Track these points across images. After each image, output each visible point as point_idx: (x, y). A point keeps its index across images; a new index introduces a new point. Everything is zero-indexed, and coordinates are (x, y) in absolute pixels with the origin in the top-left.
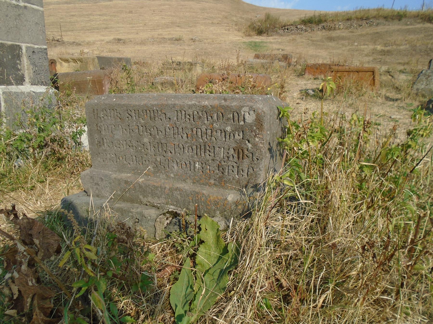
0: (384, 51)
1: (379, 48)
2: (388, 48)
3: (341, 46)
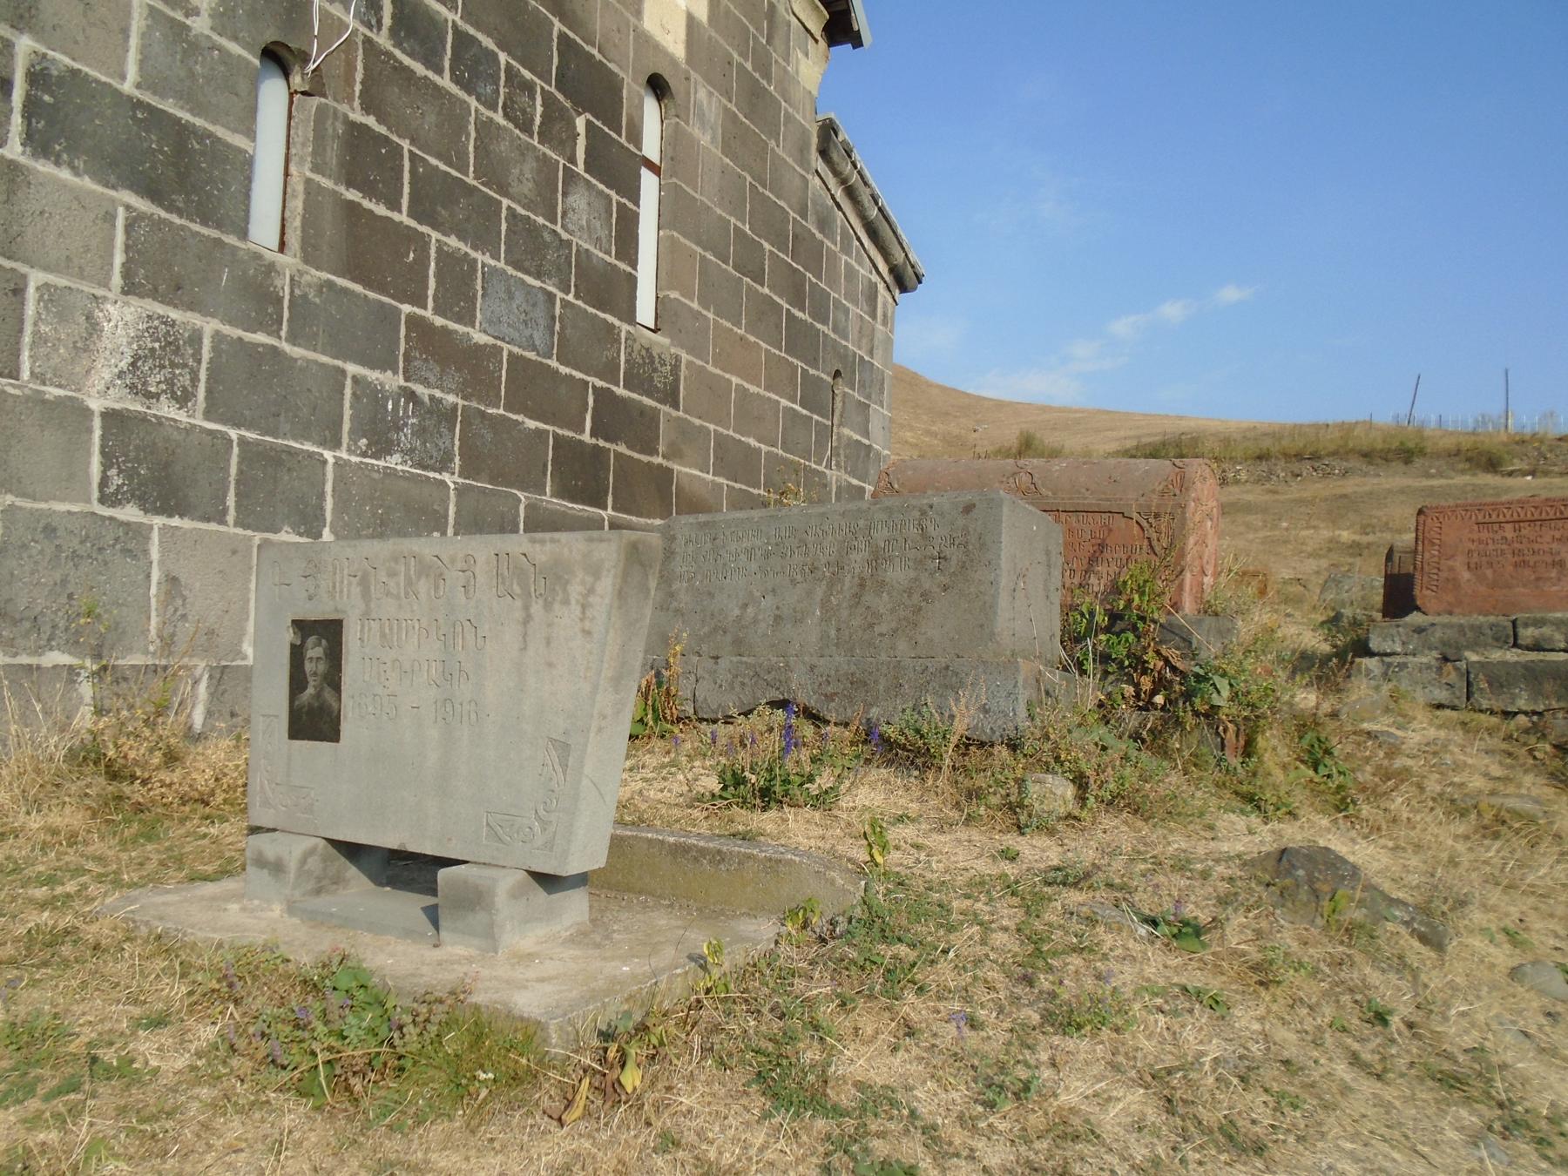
0: (1359, 544)
1: (1346, 536)
2: (1371, 538)
3: (1242, 529)
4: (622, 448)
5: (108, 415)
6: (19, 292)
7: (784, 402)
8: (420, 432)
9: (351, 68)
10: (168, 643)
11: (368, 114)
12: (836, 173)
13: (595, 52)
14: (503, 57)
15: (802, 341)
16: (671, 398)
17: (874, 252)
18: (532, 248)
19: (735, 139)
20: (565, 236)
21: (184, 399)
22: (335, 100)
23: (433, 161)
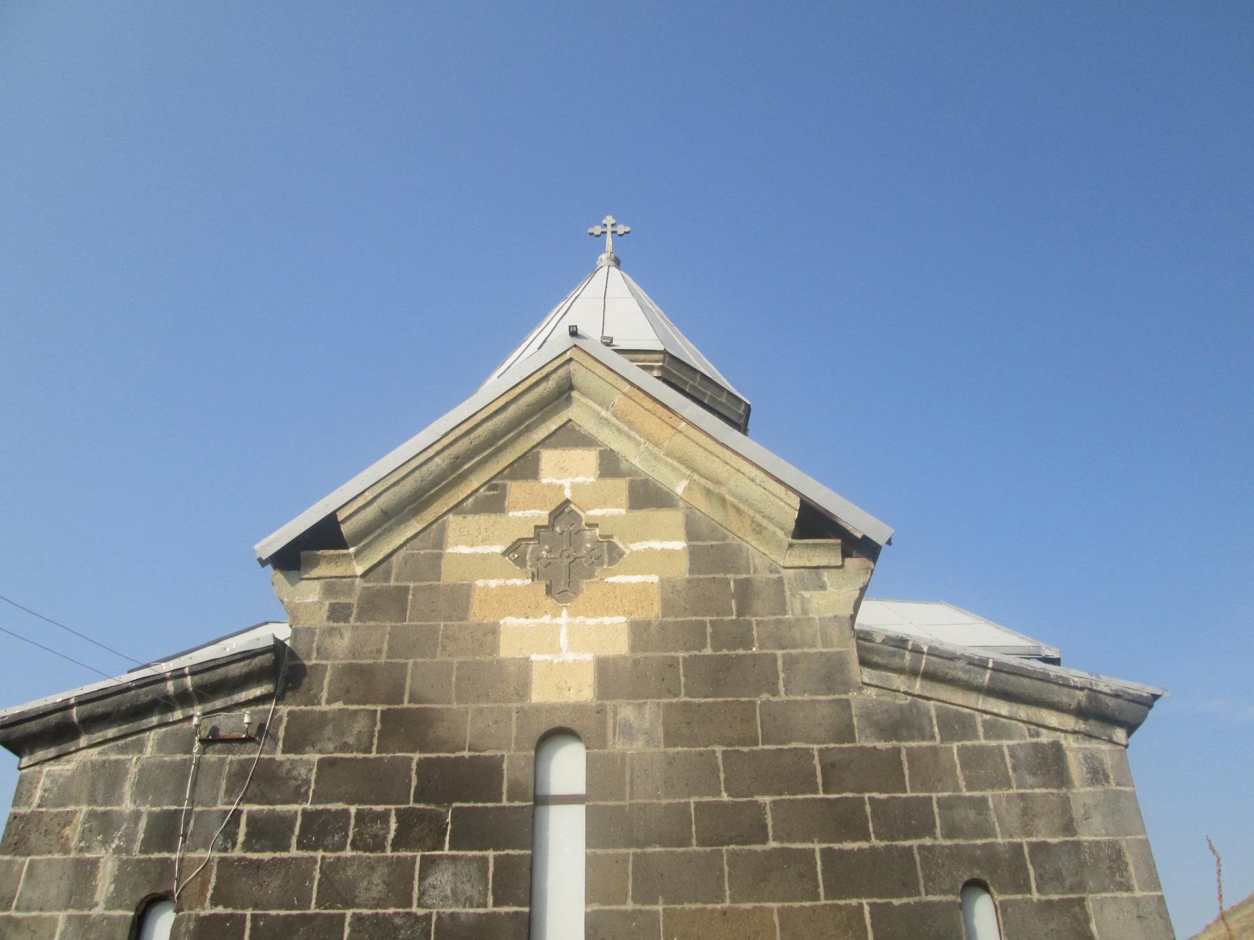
9: (205, 883)
11: (216, 905)
12: (900, 671)
13: (466, 754)
14: (353, 809)
17: (1023, 712)
20: (421, 912)
22: (190, 909)
23: (273, 912)
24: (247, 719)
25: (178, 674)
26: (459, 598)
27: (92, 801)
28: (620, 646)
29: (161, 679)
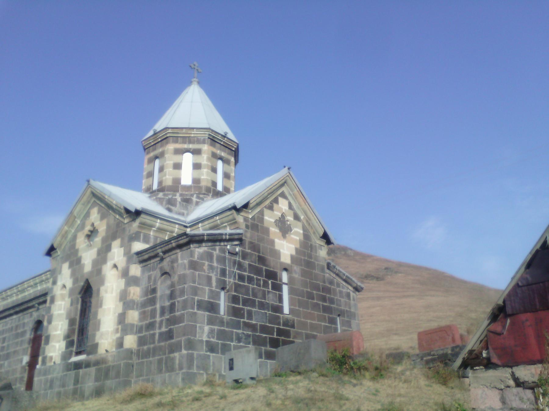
4: (283, 338)
5: (207, 341)
6: (196, 327)
7: (323, 324)
8: (245, 339)
10: (213, 370)
12: (333, 272)
13: (272, 269)
14: (255, 277)
15: (326, 310)
16: (293, 326)
17: (347, 285)
18: (262, 306)
19: (304, 274)
21: (213, 338)
24: (237, 250)
25: (226, 234)
26: (266, 231)
27: (208, 261)
28: (294, 253)
29: (221, 234)
